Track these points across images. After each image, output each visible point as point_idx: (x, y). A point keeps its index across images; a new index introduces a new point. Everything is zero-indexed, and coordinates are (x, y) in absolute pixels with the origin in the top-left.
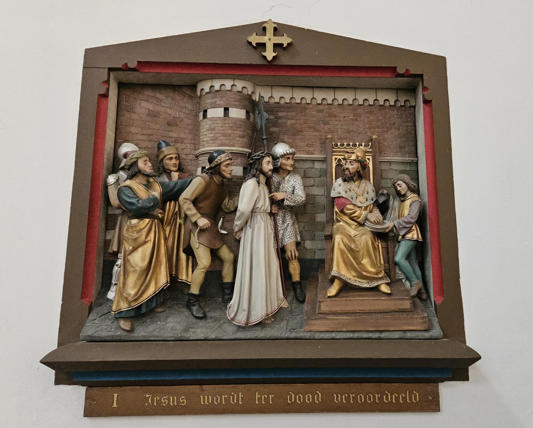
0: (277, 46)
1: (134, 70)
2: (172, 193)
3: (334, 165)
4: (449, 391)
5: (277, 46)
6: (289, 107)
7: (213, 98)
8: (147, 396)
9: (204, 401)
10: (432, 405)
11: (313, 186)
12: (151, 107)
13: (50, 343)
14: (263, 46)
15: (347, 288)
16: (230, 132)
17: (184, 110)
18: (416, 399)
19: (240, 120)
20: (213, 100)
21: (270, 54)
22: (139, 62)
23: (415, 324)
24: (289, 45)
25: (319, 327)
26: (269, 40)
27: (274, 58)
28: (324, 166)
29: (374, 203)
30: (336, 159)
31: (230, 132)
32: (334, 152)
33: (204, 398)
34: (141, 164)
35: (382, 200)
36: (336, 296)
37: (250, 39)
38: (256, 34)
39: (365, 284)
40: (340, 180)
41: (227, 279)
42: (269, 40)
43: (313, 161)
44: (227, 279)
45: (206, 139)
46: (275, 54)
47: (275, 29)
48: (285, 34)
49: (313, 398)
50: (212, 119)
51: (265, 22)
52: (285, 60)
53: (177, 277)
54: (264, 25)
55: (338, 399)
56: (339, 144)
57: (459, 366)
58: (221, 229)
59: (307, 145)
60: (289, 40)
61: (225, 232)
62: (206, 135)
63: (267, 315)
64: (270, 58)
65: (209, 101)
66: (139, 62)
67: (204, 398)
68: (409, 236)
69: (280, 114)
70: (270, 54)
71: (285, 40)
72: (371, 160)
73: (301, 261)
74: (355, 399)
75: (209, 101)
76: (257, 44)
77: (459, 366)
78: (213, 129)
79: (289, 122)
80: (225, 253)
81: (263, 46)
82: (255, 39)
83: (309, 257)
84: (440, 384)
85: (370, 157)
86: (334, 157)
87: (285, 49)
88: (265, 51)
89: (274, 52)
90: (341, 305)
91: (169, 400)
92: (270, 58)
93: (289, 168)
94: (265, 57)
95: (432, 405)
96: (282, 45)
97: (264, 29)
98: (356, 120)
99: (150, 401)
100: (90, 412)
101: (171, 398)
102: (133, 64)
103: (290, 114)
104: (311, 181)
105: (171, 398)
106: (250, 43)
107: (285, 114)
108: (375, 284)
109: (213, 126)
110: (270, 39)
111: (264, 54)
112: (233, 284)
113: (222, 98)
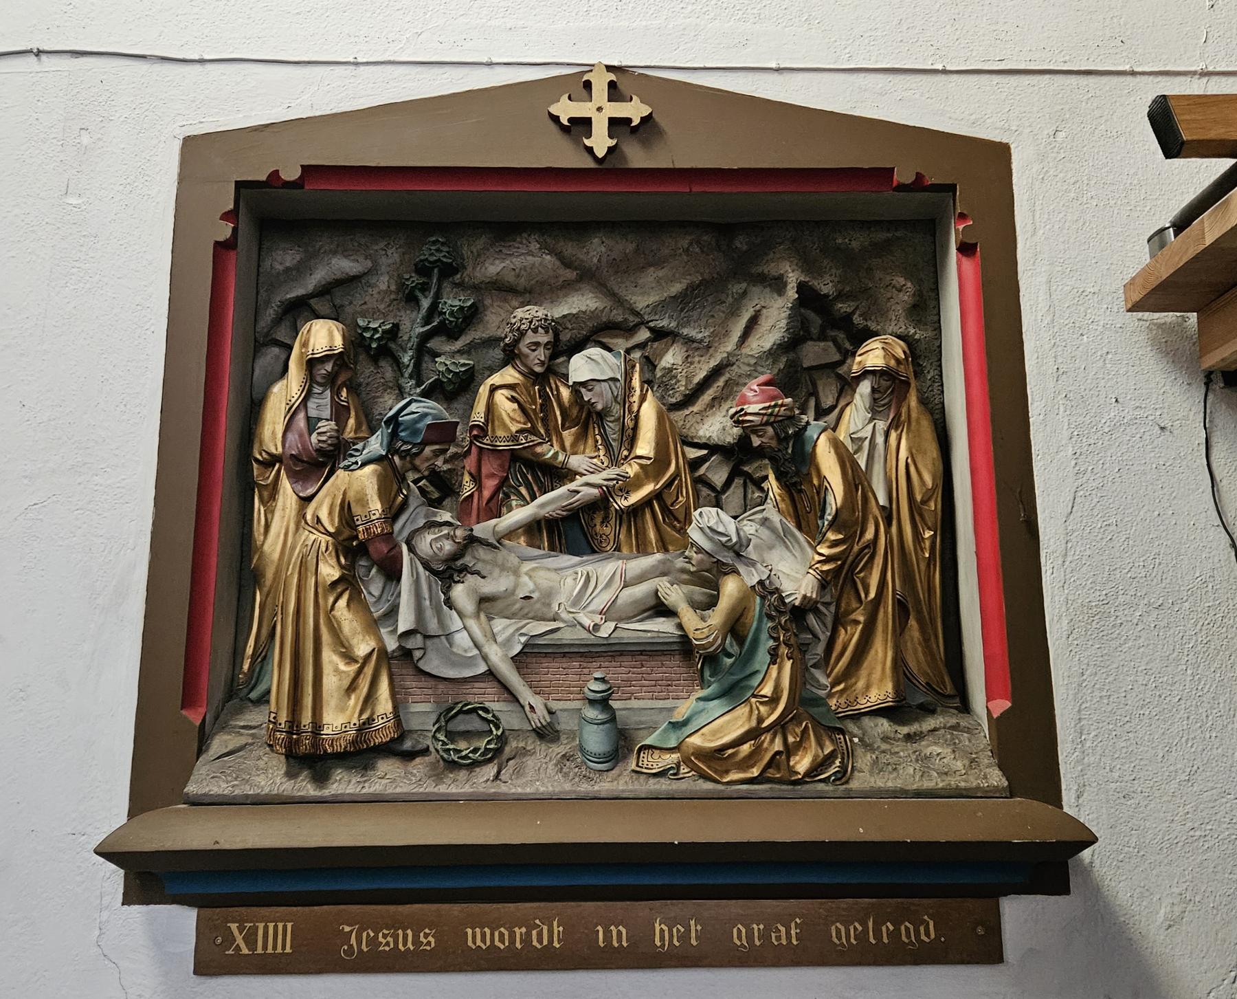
0: (616, 124)
1: (296, 185)
5: (616, 124)
8: (347, 929)
13: (110, 809)
14: (584, 124)
18: (927, 934)
21: (600, 142)
22: (305, 168)
24: (646, 120)
26: (600, 110)
27: (611, 150)
37: (554, 109)
38: (570, 98)
42: (600, 110)
46: (612, 142)
47: (612, 85)
48: (635, 97)
52: (637, 157)
54: (585, 78)
60: (645, 111)
64: (600, 152)
66: (305, 168)
70: (600, 142)
71: (635, 110)
76: (570, 120)
81: (584, 124)
82: (566, 110)
87: (635, 130)
88: (589, 136)
89: (611, 136)
92: (600, 152)
94: (590, 150)
96: (629, 120)
97: (588, 85)
99: (353, 941)
100: (211, 962)
101: (400, 932)
102: (291, 173)
105: (400, 932)
106: (555, 119)
110: (600, 109)
111: (587, 142)
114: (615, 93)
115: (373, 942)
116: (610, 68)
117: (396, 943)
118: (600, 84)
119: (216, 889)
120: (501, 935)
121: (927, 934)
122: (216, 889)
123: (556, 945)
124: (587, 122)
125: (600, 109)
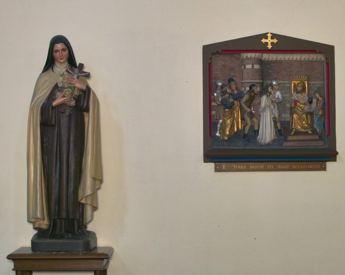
0: (272, 43)
2: (236, 98)
3: (293, 85)
4: (329, 165)
6: (276, 62)
7: (248, 61)
9: (251, 167)
10: (324, 169)
11: (285, 93)
12: (223, 63)
15: (297, 133)
16: (254, 74)
17: (236, 64)
18: (319, 167)
19: (258, 69)
20: (248, 62)
23: (320, 144)
25: (287, 145)
26: (269, 41)
28: (289, 85)
29: (307, 101)
30: (293, 83)
31: (254, 74)
32: (293, 80)
33: (251, 167)
34: (228, 91)
35: (310, 100)
36: (293, 135)
39: (303, 130)
40: (295, 93)
41: (256, 129)
42: (269, 41)
43: (285, 84)
44: (256, 129)
45: (245, 77)
49: (286, 167)
50: (247, 69)
51: (267, 33)
53: (238, 128)
55: (294, 167)
56: (295, 77)
57: (332, 156)
58: (253, 110)
59: (283, 77)
61: (254, 112)
62: (245, 76)
63: (271, 141)
65: (246, 62)
67: (251, 167)
68: (319, 113)
69: (272, 65)
70: (270, 47)
71: (275, 41)
72: (307, 83)
73: (280, 122)
74: (299, 167)
75: (246, 62)
77: (332, 156)
78: (248, 73)
79: (276, 68)
80: (255, 120)
82: (264, 41)
83: (283, 120)
84: (327, 162)
85: (306, 82)
86: (293, 82)
89: (271, 45)
90: (295, 138)
91: (241, 167)
93: (277, 89)
95: (324, 169)
98: (301, 67)
103: (276, 65)
104: (284, 92)
107: (274, 65)
108: (306, 130)
109: (248, 72)
110: (269, 41)
112: (258, 131)
113: (251, 61)
114: (272, 38)
115: (237, 168)
116: (271, 33)
117: (241, 168)
118: (269, 35)
119: (216, 160)
120: (256, 167)
121: (319, 167)
122: (216, 160)
123: (263, 168)
124: (267, 43)
125: (269, 41)
